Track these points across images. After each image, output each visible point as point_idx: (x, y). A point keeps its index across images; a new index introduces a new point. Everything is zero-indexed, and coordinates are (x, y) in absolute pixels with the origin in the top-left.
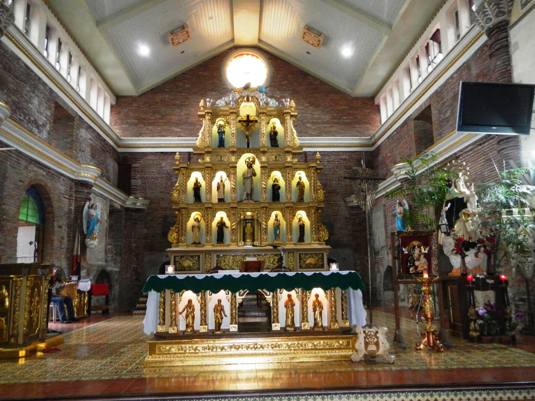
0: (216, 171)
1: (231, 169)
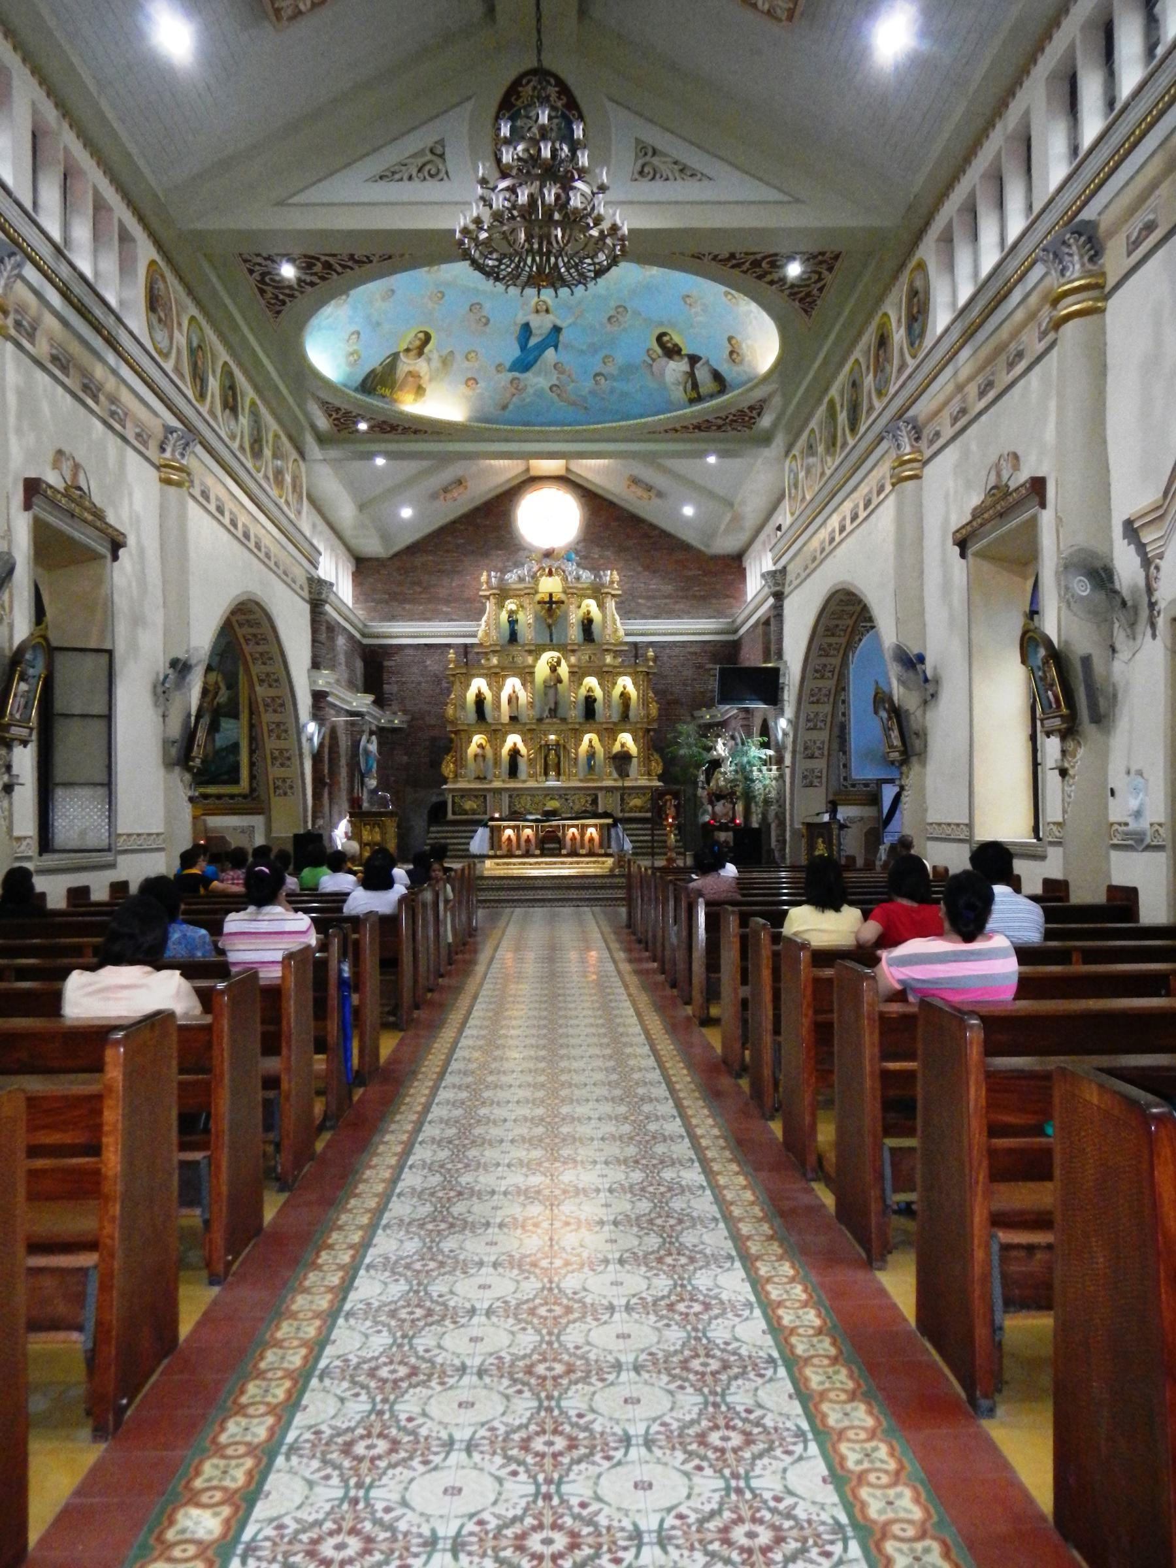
0: (505, 677)
1: (527, 675)
